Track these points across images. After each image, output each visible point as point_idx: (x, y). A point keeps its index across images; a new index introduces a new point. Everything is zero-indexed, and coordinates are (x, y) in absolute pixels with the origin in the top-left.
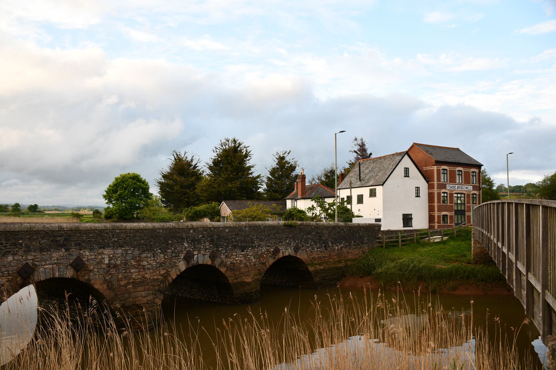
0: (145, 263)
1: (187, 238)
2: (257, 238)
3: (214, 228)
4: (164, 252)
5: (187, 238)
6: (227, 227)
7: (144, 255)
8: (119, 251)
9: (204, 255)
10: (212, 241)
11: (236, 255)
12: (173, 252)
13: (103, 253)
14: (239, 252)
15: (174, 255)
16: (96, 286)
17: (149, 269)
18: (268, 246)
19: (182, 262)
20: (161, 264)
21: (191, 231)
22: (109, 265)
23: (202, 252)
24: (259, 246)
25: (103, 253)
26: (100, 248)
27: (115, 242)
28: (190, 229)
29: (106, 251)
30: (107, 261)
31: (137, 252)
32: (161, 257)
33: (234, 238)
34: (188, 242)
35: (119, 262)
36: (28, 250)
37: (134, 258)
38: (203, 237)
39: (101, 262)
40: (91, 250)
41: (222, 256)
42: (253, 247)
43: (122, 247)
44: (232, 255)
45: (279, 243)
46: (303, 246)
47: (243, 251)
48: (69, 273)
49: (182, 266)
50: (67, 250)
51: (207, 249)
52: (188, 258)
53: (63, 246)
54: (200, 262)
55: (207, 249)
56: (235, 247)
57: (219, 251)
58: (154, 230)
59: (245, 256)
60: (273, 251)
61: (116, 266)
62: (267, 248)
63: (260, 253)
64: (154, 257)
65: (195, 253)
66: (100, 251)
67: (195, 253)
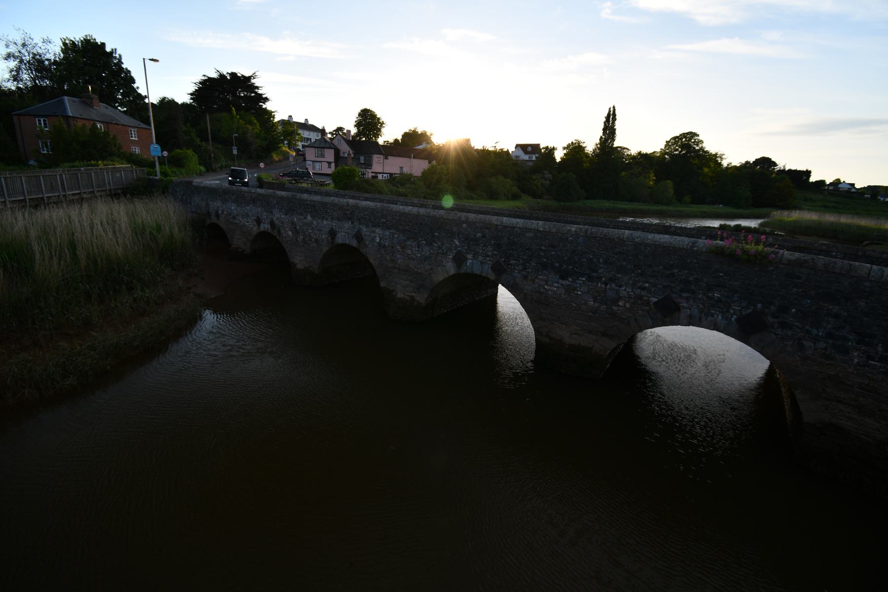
0: (409, 252)
3: (506, 227)
6: (530, 230)
7: (409, 243)
8: (387, 233)
9: (482, 263)
11: (547, 282)
13: (374, 232)
15: (440, 251)
16: (371, 261)
18: (644, 289)
21: (464, 226)
22: (379, 244)
23: (480, 258)
24: (612, 280)
25: (374, 232)
26: (373, 226)
28: (464, 222)
29: (378, 230)
32: (427, 251)
34: (459, 240)
35: (387, 244)
36: (332, 219)
38: (484, 236)
39: (373, 239)
40: (367, 226)
41: (516, 274)
43: (389, 229)
44: (536, 278)
47: (563, 278)
48: (354, 243)
49: (451, 268)
50: (352, 223)
51: (488, 256)
52: (459, 260)
54: (477, 270)
55: (488, 256)
57: (511, 265)
60: (655, 303)
61: (384, 246)
62: (638, 291)
64: (419, 247)
65: (469, 256)
66: (373, 229)
67: (469, 256)
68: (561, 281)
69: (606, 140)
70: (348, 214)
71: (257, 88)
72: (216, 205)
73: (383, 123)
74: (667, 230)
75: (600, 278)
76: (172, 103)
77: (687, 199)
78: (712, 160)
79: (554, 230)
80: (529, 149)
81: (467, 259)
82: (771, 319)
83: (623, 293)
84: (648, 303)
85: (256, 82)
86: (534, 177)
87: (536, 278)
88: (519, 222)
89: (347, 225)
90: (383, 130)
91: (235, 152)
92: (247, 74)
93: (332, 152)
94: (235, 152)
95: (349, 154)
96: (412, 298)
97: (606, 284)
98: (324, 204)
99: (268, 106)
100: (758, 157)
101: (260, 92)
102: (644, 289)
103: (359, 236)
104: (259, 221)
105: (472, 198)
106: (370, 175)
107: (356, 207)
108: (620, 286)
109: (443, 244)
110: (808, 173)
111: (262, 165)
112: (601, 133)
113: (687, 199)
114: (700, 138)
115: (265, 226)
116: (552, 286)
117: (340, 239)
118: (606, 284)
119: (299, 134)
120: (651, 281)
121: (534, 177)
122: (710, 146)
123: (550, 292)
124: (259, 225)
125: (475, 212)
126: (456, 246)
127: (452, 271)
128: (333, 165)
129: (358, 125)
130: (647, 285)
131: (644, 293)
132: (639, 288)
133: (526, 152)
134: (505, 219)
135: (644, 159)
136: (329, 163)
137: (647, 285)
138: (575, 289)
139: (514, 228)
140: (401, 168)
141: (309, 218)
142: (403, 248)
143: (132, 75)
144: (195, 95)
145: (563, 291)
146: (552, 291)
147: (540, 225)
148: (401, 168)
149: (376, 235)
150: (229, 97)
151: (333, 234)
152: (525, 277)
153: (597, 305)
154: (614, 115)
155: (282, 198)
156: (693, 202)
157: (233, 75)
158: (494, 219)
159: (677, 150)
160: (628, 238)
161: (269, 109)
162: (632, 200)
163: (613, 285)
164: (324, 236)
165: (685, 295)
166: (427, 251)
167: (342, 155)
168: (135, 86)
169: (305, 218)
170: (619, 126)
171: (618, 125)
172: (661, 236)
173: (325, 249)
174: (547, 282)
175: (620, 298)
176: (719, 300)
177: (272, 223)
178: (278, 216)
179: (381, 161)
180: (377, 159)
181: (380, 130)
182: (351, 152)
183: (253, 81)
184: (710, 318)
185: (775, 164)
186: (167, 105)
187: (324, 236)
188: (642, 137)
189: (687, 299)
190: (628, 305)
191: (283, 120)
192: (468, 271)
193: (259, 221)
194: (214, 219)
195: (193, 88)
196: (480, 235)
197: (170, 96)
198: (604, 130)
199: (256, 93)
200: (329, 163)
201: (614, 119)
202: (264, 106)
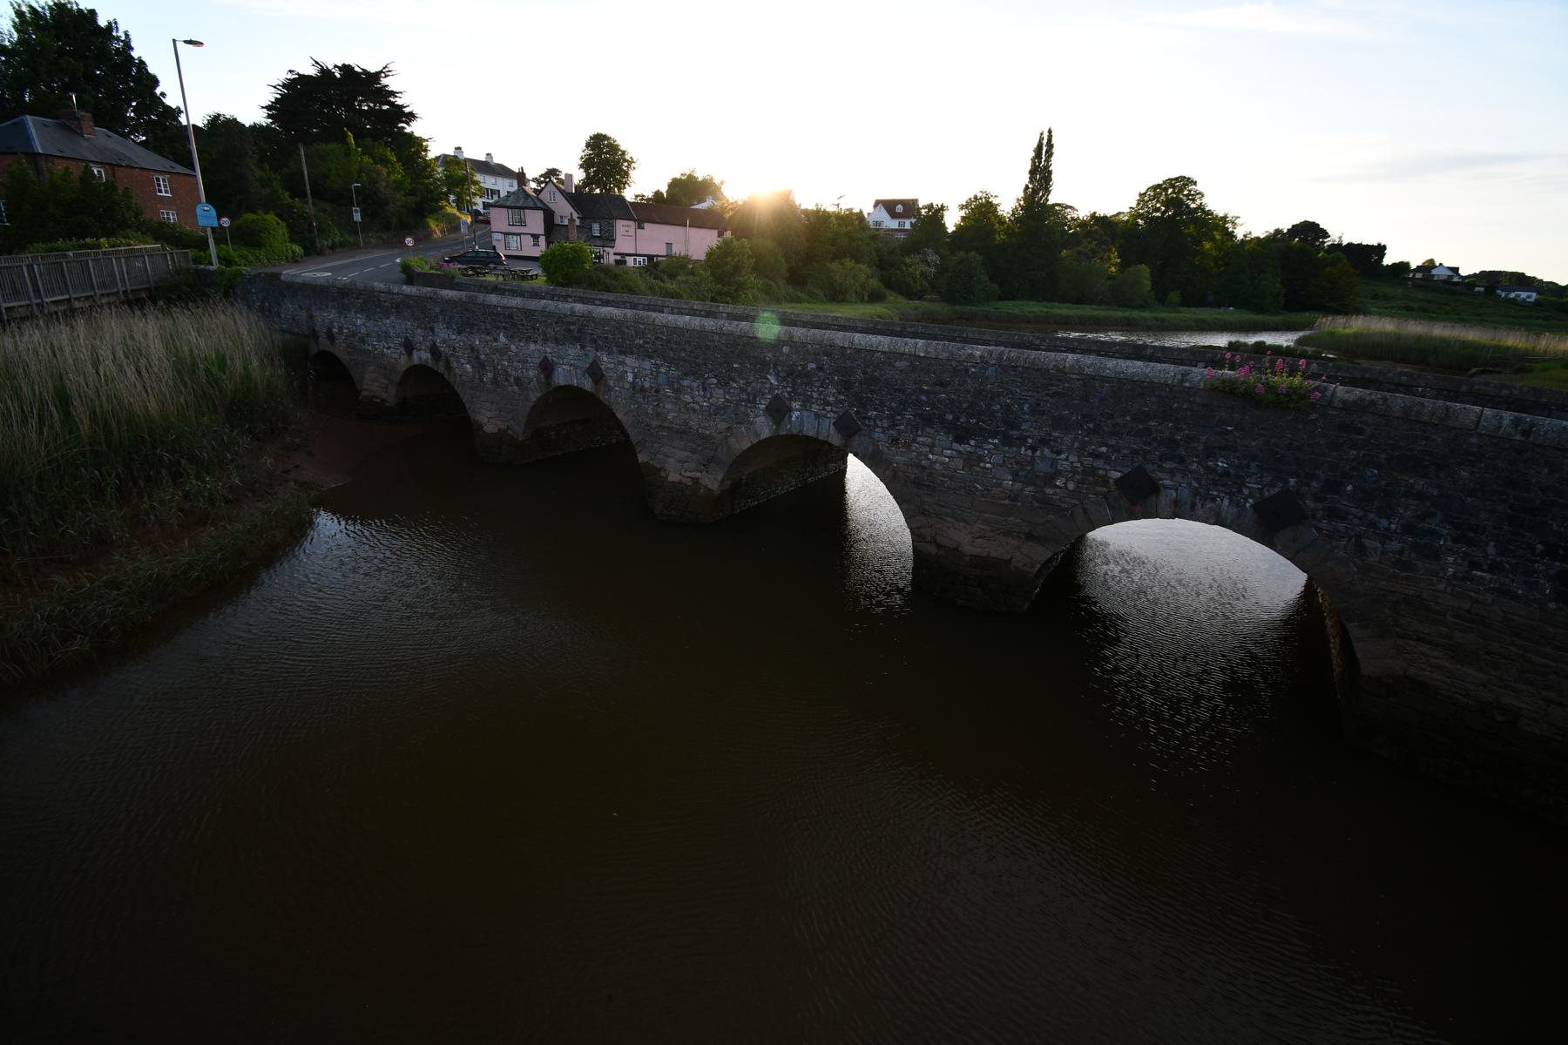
0: (688, 398)
1: (776, 365)
2: (1033, 411)
3: (859, 351)
4: (724, 383)
5: (776, 365)
7: (686, 383)
8: (647, 364)
9: (818, 416)
10: (846, 386)
11: (932, 446)
12: (742, 390)
14: (942, 438)
16: (620, 416)
17: (695, 411)
18: (1098, 456)
19: (762, 419)
20: (718, 410)
21: (786, 349)
23: (815, 408)
24: (1044, 442)
25: (623, 363)
26: (621, 353)
27: (641, 346)
28: (785, 343)
29: (630, 360)
30: (630, 379)
31: (674, 373)
32: (719, 397)
33: (926, 393)
35: (647, 385)
36: (546, 340)
37: (669, 383)
38: (820, 369)
39: (622, 377)
40: (610, 353)
41: (878, 434)
42: (1007, 440)
44: (914, 441)
45: (1163, 458)
46: (1333, 514)
47: (959, 439)
48: (588, 384)
49: (764, 427)
50: (583, 347)
51: (828, 404)
52: (778, 411)
53: (577, 339)
55: (828, 404)
56: (927, 420)
57: (869, 418)
58: (702, 333)
59: (971, 461)
60: (1117, 481)
61: (643, 390)
62: (1089, 461)
63: (1042, 467)
64: (704, 389)
66: (622, 357)
68: (956, 446)
69: (1035, 191)
70: (574, 331)
71: (393, 94)
72: (326, 317)
73: (630, 162)
74: (1138, 353)
75: (1023, 439)
76: (233, 124)
77: (1174, 296)
78: (1216, 227)
79: (945, 355)
80: (899, 208)
81: (790, 410)
82: (1310, 504)
83: (1063, 465)
84: (1105, 480)
85: (390, 83)
86: (908, 260)
87: (914, 441)
88: (883, 342)
89: (573, 351)
90: (632, 173)
91: (357, 217)
92: (373, 69)
93: (540, 214)
94: (357, 217)
95: (571, 220)
96: (696, 481)
97: (1034, 450)
98: (528, 313)
99: (415, 128)
100: (1297, 222)
101: (399, 102)
102: (1098, 456)
103: (595, 372)
104: (409, 347)
105: (799, 300)
106: (612, 259)
107: (588, 317)
108: (1059, 453)
109: (748, 384)
110: (1380, 250)
111: (409, 241)
112: (1025, 179)
113: (1174, 296)
114: (1199, 187)
115: (422, 356)
116: (941, 454)
117: (562, 377)
118: (1034, 450)
119: (476, 183)
120: (1112, 442)
121: (908, 260)
122: (1216, 201)
123: (938, 466)
124: (410, 354)
125: (805, 324)
126: (772, 388)
127: (766, 433)
128: (542, 240)
129: (586, 164)
130: (1104, 449)
131: (1099, 463)
132: (1091, 455)
133: (894, 215)
134: (858, 337)
135: (1101, 224)
136: (536, 237)
137: (1104, 449)
138: (981, 459)
139: (873, 352)
140: (669, 245)
141: (502, 339)
142: (677, 391)
143: (151, 70)
144: (276, 109)
145: (959, 463)
146: (942, 464)
147: (919, 346)
148: (669, 245)
149: (627, 370)
150: (340, 113)
151: (547, 367)
152: (895, 441)
153: (1018, 486)
154: (1050, 145)
155: (449, 301)
156: (1183, 304)
157: (346, 69)
158: (839, 337)
159: (1158, 210)
160: (1072, 367)
161: (417, 134)
162: (1079, 300)
163: (1047, 451)
164: (531, 373)
165: (1168, 465)
166: (719, 397)
167: (558, 221)
168: (158, 91)
169: (496, 340)
170: (1059, 166)
171: (1056, 165)
172: (1129, 363)
173: (535, 396)
174: (932, 446)
175: (1057, 474)
176: (1226, 474)
177: (434, 351)
178: (444, 335)
179: (632, 231)
180: (623, 228)
181: (627, 174)
182: (575, 215)
183: (384, 81)
184: (1209, 505)
185: (1325, 234)
186: (222, 128)
187: (531, 373)
188: (1098, 188)
189: (1172, 472)
190: (1071, 486)
191: (445, 156)
192: (795, 432)
193: (409, 347)
194: (324, 344)
195: (270, 96)
196: (813, 366)
197: (228, 111)
198: (1032, 172)
199: (392, 104)
200: (536, 237)
201: (1050, 154)
202: (408, 130)
